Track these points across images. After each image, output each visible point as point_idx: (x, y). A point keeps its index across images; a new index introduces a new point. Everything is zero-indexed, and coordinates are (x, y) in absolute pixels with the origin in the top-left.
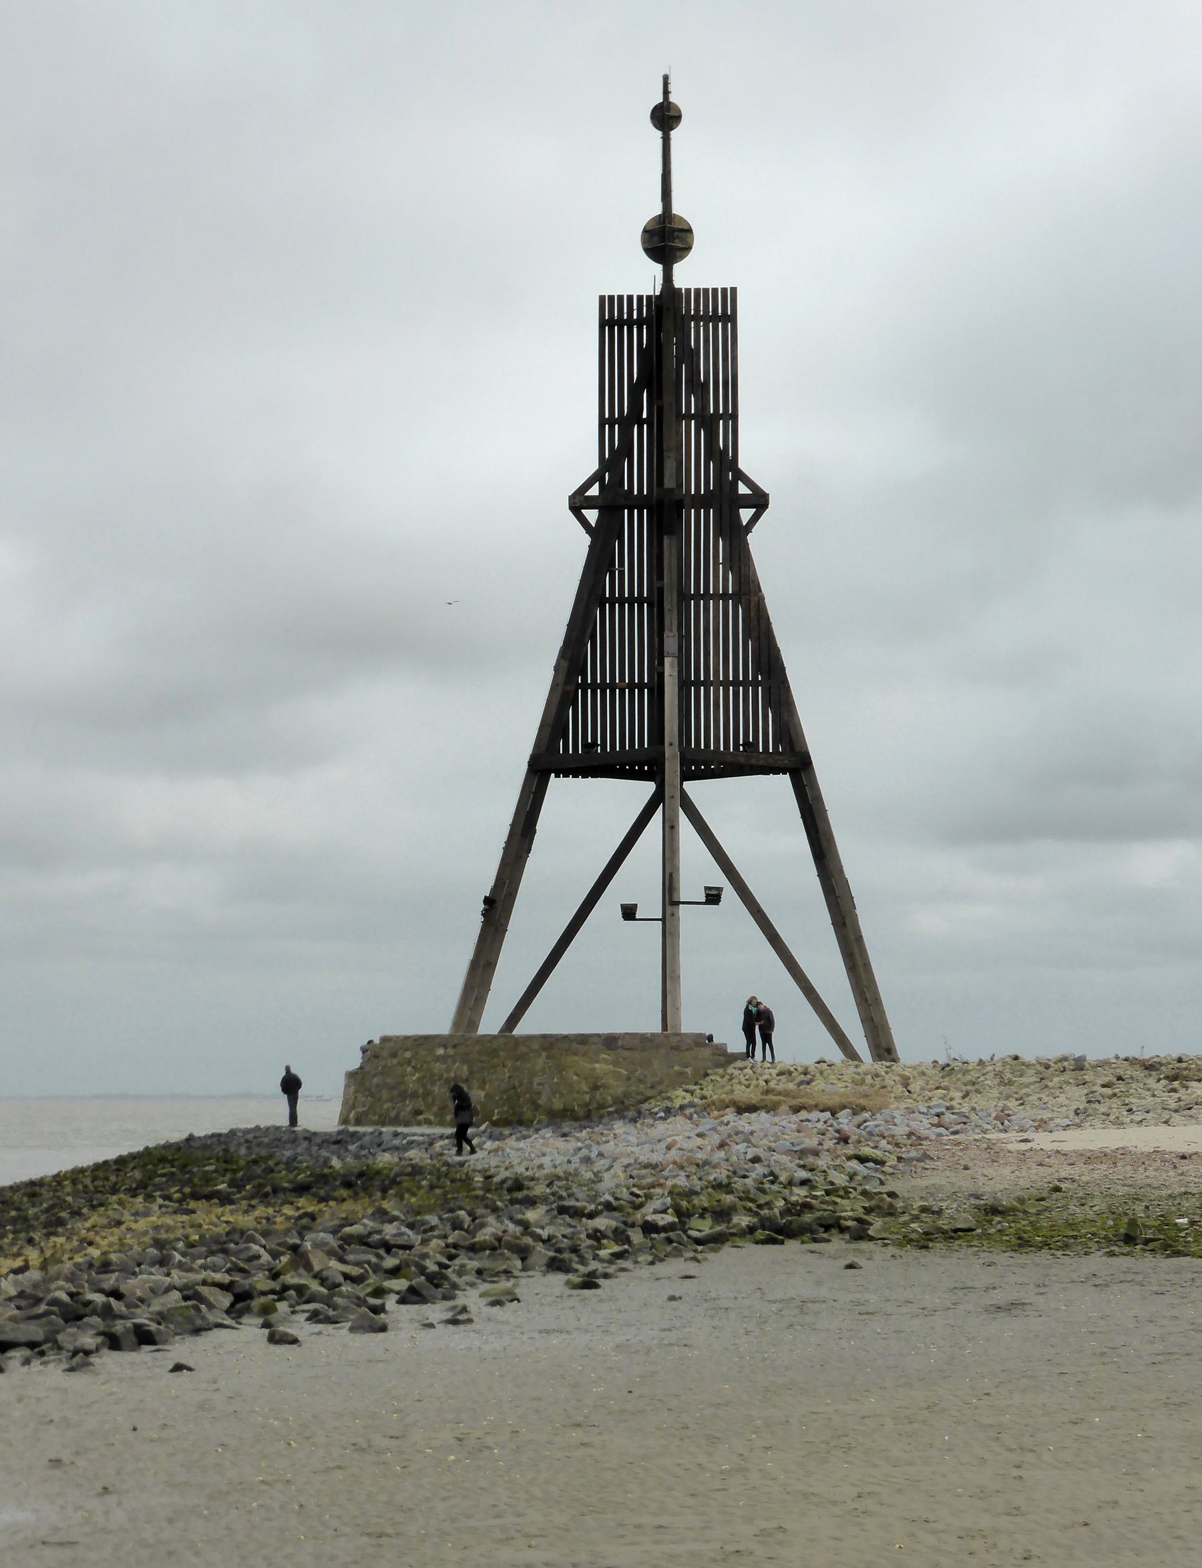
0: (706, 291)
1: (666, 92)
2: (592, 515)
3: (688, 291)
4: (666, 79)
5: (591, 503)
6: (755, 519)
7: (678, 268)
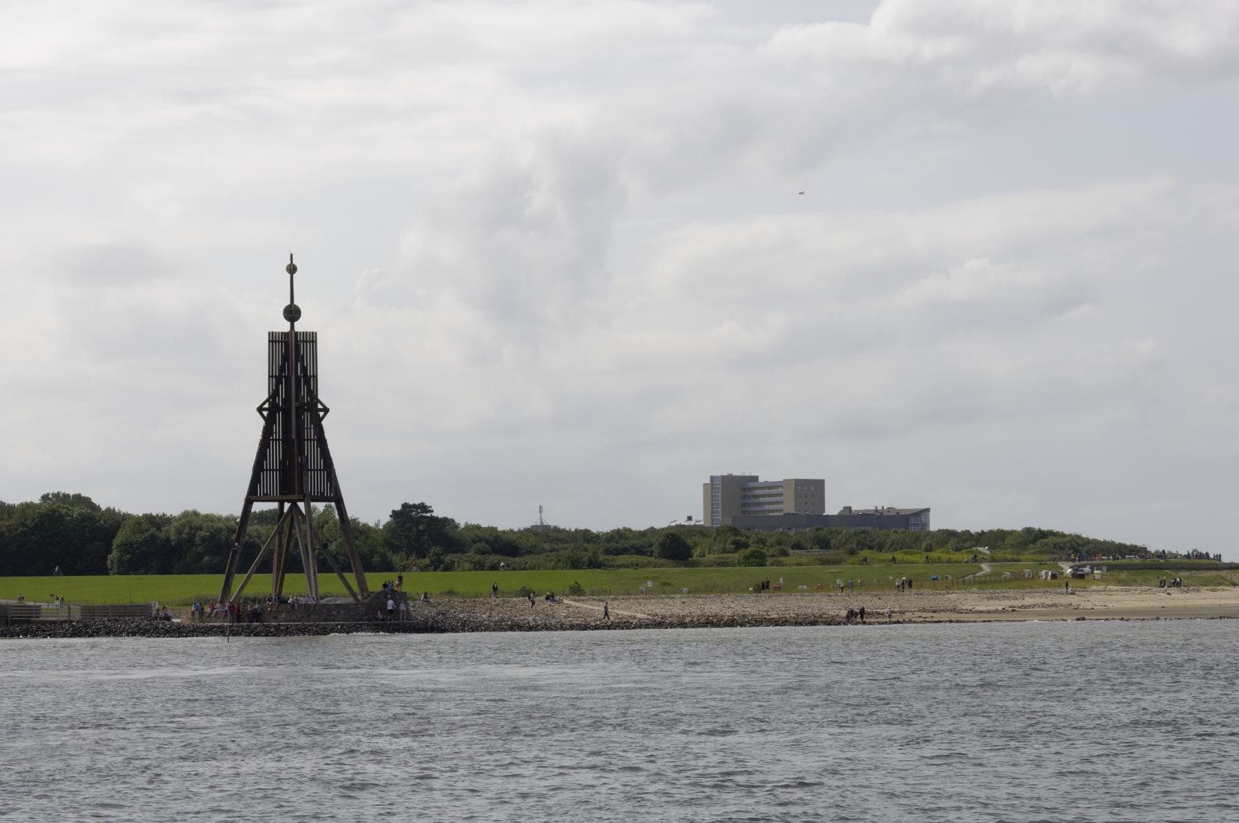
0: (307, 333)
2: (265, 413)
3: (300, 333)
4: (292, 256)
5: (265, 409)
7: (296, 324)
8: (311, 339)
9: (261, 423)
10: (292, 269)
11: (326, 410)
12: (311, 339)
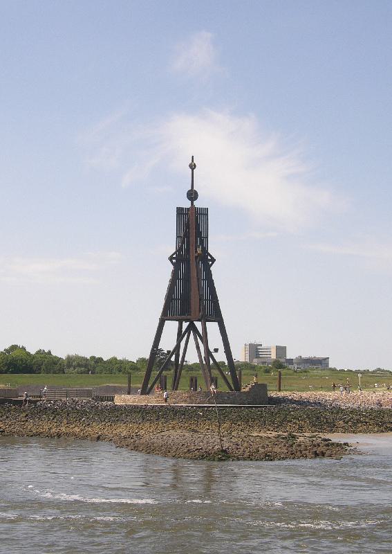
1: (193, 161)
5: (174, 258)
6: (212, 265)
8: (204, 212)
9: (171, 268)
10: (193, 167)
11: (213, 260)
12: (204, 212)
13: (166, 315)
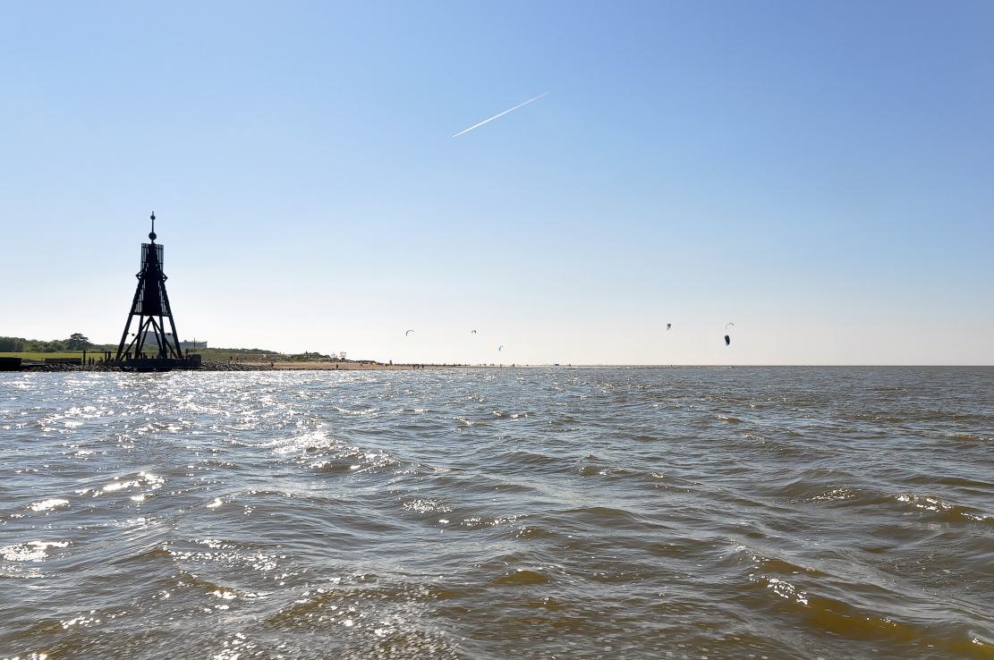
8: (161, 248)
9: (137, 281)
10: (153, 218)
11: (166, 278)
13: (132, 313)
